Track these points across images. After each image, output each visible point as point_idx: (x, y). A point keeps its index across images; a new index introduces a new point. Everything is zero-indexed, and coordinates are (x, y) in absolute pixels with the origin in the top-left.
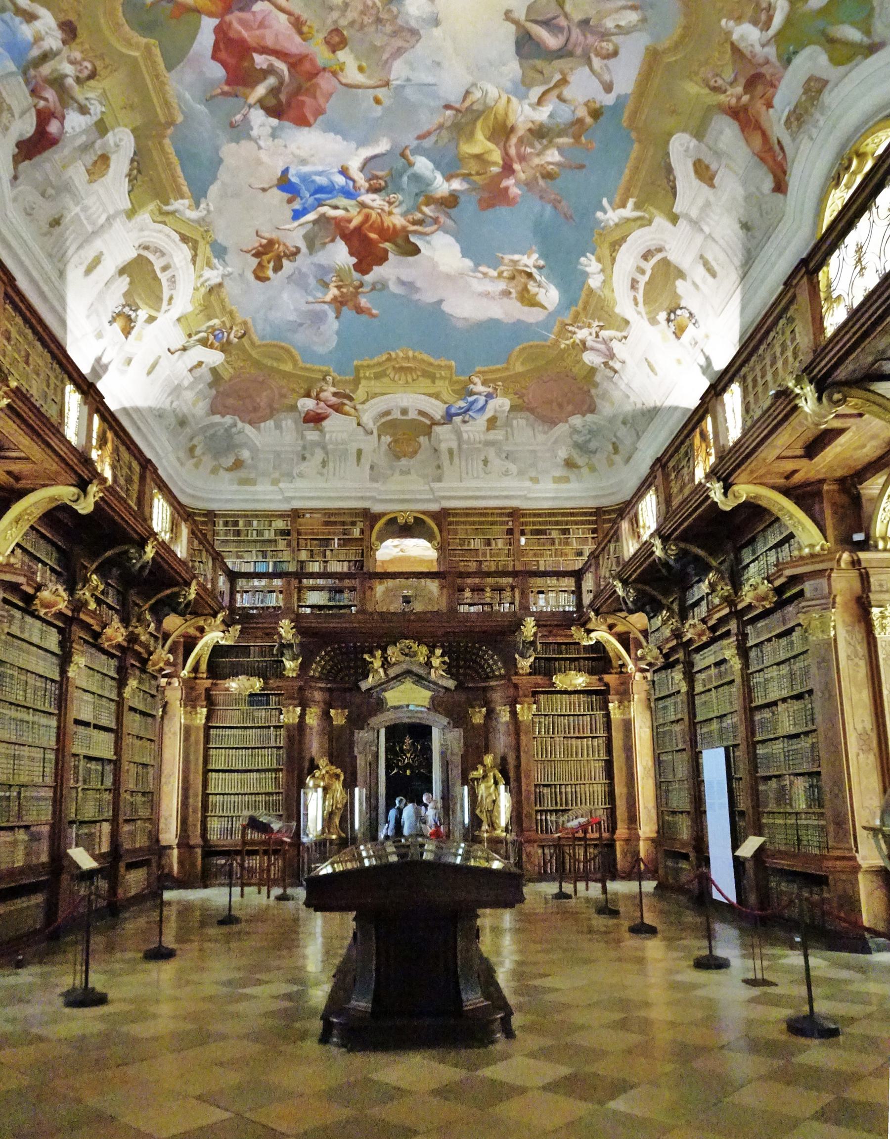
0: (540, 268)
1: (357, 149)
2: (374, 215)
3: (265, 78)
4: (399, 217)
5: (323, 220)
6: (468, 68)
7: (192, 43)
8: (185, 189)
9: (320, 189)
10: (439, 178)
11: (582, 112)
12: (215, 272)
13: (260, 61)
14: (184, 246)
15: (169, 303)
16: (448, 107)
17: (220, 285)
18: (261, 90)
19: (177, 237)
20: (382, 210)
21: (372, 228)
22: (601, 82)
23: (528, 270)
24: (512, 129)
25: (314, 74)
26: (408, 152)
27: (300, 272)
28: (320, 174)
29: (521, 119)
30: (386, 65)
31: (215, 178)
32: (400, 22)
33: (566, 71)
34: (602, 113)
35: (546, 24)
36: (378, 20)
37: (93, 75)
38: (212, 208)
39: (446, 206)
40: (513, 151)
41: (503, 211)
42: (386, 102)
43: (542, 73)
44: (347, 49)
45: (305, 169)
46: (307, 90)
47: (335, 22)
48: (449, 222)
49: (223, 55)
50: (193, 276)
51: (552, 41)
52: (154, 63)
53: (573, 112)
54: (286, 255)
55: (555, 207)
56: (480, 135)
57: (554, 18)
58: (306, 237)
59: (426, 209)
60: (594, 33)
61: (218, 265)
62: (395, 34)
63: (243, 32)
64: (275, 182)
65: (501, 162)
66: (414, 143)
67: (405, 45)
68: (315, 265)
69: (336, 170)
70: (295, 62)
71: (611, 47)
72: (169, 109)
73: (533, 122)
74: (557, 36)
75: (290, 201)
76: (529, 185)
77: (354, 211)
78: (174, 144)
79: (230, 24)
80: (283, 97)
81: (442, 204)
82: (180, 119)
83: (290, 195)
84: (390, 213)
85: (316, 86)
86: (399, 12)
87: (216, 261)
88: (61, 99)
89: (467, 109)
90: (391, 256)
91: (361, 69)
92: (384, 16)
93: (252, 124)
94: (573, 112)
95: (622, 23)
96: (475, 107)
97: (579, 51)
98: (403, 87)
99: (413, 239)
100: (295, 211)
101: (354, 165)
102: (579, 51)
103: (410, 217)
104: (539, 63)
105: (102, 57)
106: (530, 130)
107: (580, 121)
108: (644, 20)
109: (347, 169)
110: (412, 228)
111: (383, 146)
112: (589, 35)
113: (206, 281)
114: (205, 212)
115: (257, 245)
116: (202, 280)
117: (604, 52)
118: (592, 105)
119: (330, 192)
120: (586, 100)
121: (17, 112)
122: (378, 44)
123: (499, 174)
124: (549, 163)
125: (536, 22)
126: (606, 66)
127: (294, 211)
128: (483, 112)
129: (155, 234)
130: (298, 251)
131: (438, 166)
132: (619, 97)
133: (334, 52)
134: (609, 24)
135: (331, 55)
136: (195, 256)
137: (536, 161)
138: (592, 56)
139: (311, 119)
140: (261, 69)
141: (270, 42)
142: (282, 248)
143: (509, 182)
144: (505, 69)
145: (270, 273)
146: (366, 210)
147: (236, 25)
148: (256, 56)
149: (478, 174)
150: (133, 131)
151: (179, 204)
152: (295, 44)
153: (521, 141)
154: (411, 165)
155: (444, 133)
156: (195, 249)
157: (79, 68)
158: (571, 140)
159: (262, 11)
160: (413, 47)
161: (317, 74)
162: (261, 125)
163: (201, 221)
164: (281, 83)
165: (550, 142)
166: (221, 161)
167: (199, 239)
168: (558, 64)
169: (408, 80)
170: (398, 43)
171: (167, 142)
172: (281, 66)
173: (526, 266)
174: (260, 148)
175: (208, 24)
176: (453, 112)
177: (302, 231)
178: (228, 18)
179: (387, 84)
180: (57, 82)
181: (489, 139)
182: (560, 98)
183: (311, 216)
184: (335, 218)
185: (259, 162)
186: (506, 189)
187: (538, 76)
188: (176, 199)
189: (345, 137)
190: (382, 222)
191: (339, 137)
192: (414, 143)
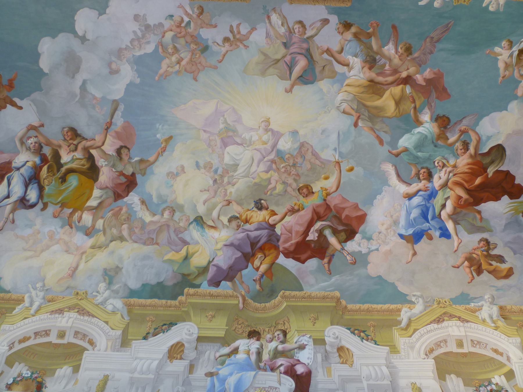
0: (511, 44)
1: (389, 186)
2: (456, 179)
3: (325, 237)
4: (458, 160)
5: (454, 217)
6: (325, 112)
7: (291, 273)
8: (393, 306)
9: (424, 215)
10: (420, 129)
11: (349, 35)
12: (486, 308)
13: (312, 236)
14: (445, 324)
15: (501, 354)
16: (356, 125)
17: (501, 308)
18: (333, 240)
19: (436, 326)
20: (450, 172)
21: (470, 181)
22: (323, 27)
23: (516, 53)
24: (371, 81)
25: (328, 207)
26: (394, 152)
27: (509, 242)
28: (409, 213)
29: (362, 75)
30: (324, 163)
31: (393, 284)
32: (295, 153)
33: (320, 51)
34: (346, 22)
35: (291, 68)
36: (294, 165)
37: (285, 333)
38: (418, 294)
39: (448, 125)
40: (390, 79)
41: (448, 81)
42: (352, 163)
43: (324, 66)
44: (312, 185)
45: (402, 222)
46: (337, 212)
47: (294, 190)
48: (465, 122)
49: (303, 257)
50: (480, 327)
51: (302, 63)
52: (294, 297)
53: (350, 41)
54: (487, 251)
55: (438, 41)
56: (379, 103)
57: (287, 63)
58: (470, 232)
59: (452, 140)
60: (291, 38)
61: (480, 304)
62: (303, 157)
63: (292, 242)
64: (409, 245)
65: (401, 87)
66: (386, 147)
67: (310, 151)
68: (504, 230)
69: (407, 202)
70: (317, 216)
71: (297, 26)
72: (327, 298)
73: (363, 68)
74: (298, 61)
75: (431, 238)
76: (420, 64)
77: (449, 193)
78: (354, 302)
79: (285, 249)
80: (340, 228)
81: (445, 127)
82: (338, 294)
83: (425, 237)
84: (455, 166)
85: (335, 206)
86: (289, 154)
87: (472, 305)
88: (287, 357)
89: (356, 112)
90: (504, 168)
91: (326, 178)
92: (291, 162)
93: (356, 250)
94: (350, 41)
95: (280, 23)
96: (356, 107)
97: (305, 46)
98: (340, 154)
99: (485, 150)
100: (441, 236)
101: (403, 189)
102: (305, 46)
103: (459, 152)
104: (318, 69)
105: (277, 324)
106: (370, 68)
107: (356, 35)
108: (274, 9)
109: (407, 194)
110: (472, 150)
111: (389, 169)
112: (293, 41)
113: (491, 317)
114: (420, 299)
115: (468, 270)
116: (488, 320)
117: (301, 30)
118: (341, 30)
119: (428, 209)
120: (338, 34)
121: (276, 385)
122: (309, 166)
123: (412, 86)
124: (397, 52)
125: (291, 74)
126: (310, 26)
127: (440, 237)
128: (358, 101)
129: (422, 340)
130: (487, 242)
131: (408, 131)
132: (330, 13)
133: (313, 193)
134: (282, 30)
135: (315, 195)
136: (459, 318)
137: (396, 61)
138: (305, 37)
139: (360, 213)
140: (318, 237)
141: (302, 229)
142: (479, 253)
143: (419, 78)
144: (325, 90)
145: (504, 267)
146: (449, 184)
147: (287, 245)
148: (308, 239)
149: (414, 101)
150: (332, 324)
151: (405, 315)
152: (306, 215)
153: (378, 74)
154: (406, 150)
155: (377, 127)
156: (451, 317)
157: (276, 338)
158: (373, 38)
159: (281, 230)
160: (312, 147)
161: (327, 204)
162: (359, 245)
163: (427, 304)
164: (330, 227)
165: (377, 53)
166: (380, 277)
167: (444, 310)
168: (316, 56)
169: (335, 150)
170: (309, 156)
171: (350, 306)
172: (318, 225)
173: (511, 56)
174: (377, 250)
175: (282, 260)
176: (360, 121)
177: (463, 234)
178: (281, 249)
179: (338, 163)
180: (277, 354)
181: (382, 96)
182: (341, 51)
183: (450, 226)
184: (455, 208)
185: (390, 252)
186: (426, 80)
187: (327, 68)
188: (400, 315)
189: (379, 192)
190: (466, 173)
191: (378, 197)
192: (386, 147)
